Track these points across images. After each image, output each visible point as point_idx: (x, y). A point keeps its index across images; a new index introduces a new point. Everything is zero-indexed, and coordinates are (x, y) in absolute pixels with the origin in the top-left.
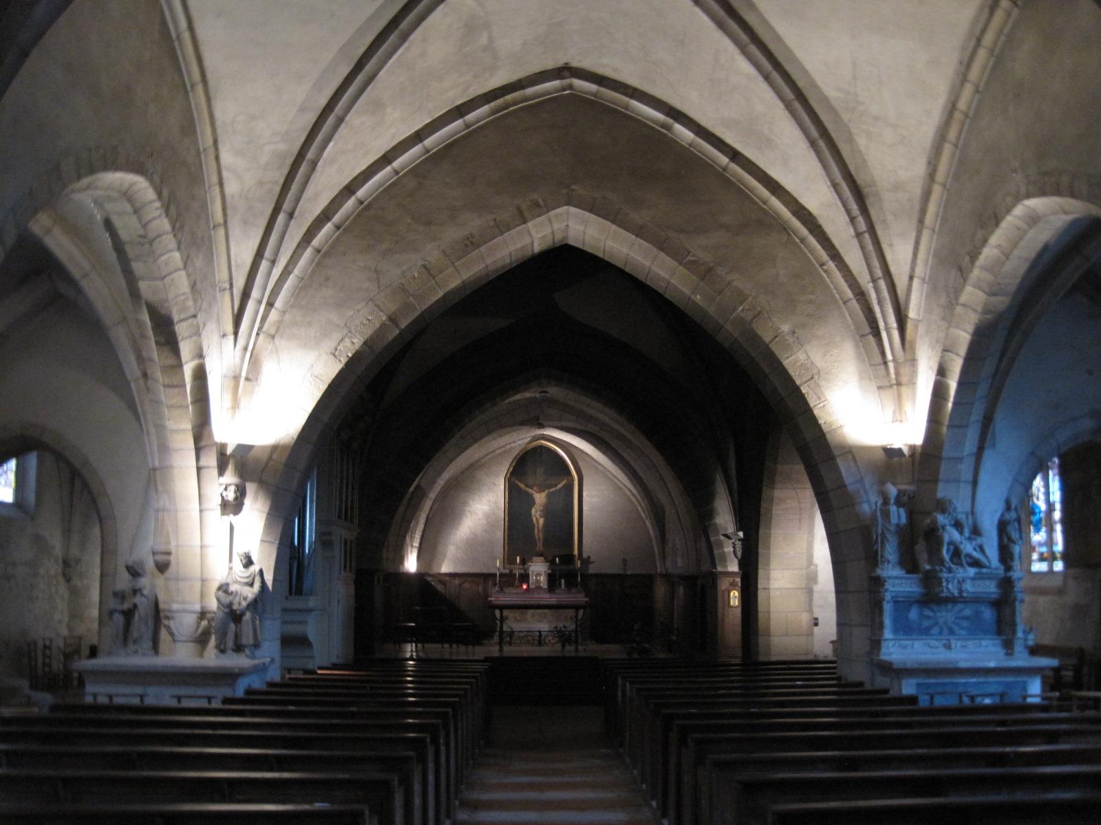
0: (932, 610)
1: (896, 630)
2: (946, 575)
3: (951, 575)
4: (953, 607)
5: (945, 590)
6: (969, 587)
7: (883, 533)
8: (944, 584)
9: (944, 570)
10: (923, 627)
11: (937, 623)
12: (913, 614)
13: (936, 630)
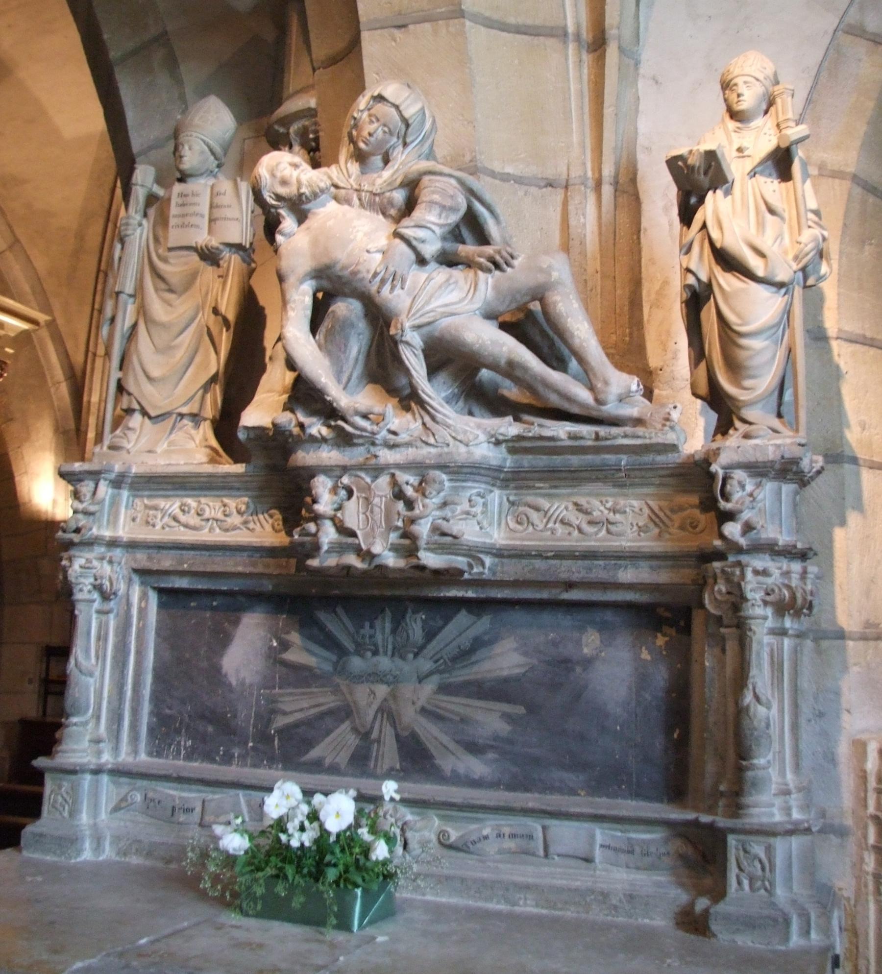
0: (330, 642)
1: (164, 731)
2: (328, 455)
3: (355, 455)
4: (430, 635)
5: (328, 535)
6: (482, 524)
7: (139, 293)
8: (325, 504)
9: (317, 428)
10: (280, 722)
11: (344, 712)
12: (246, 650)
13: (338, 743)
